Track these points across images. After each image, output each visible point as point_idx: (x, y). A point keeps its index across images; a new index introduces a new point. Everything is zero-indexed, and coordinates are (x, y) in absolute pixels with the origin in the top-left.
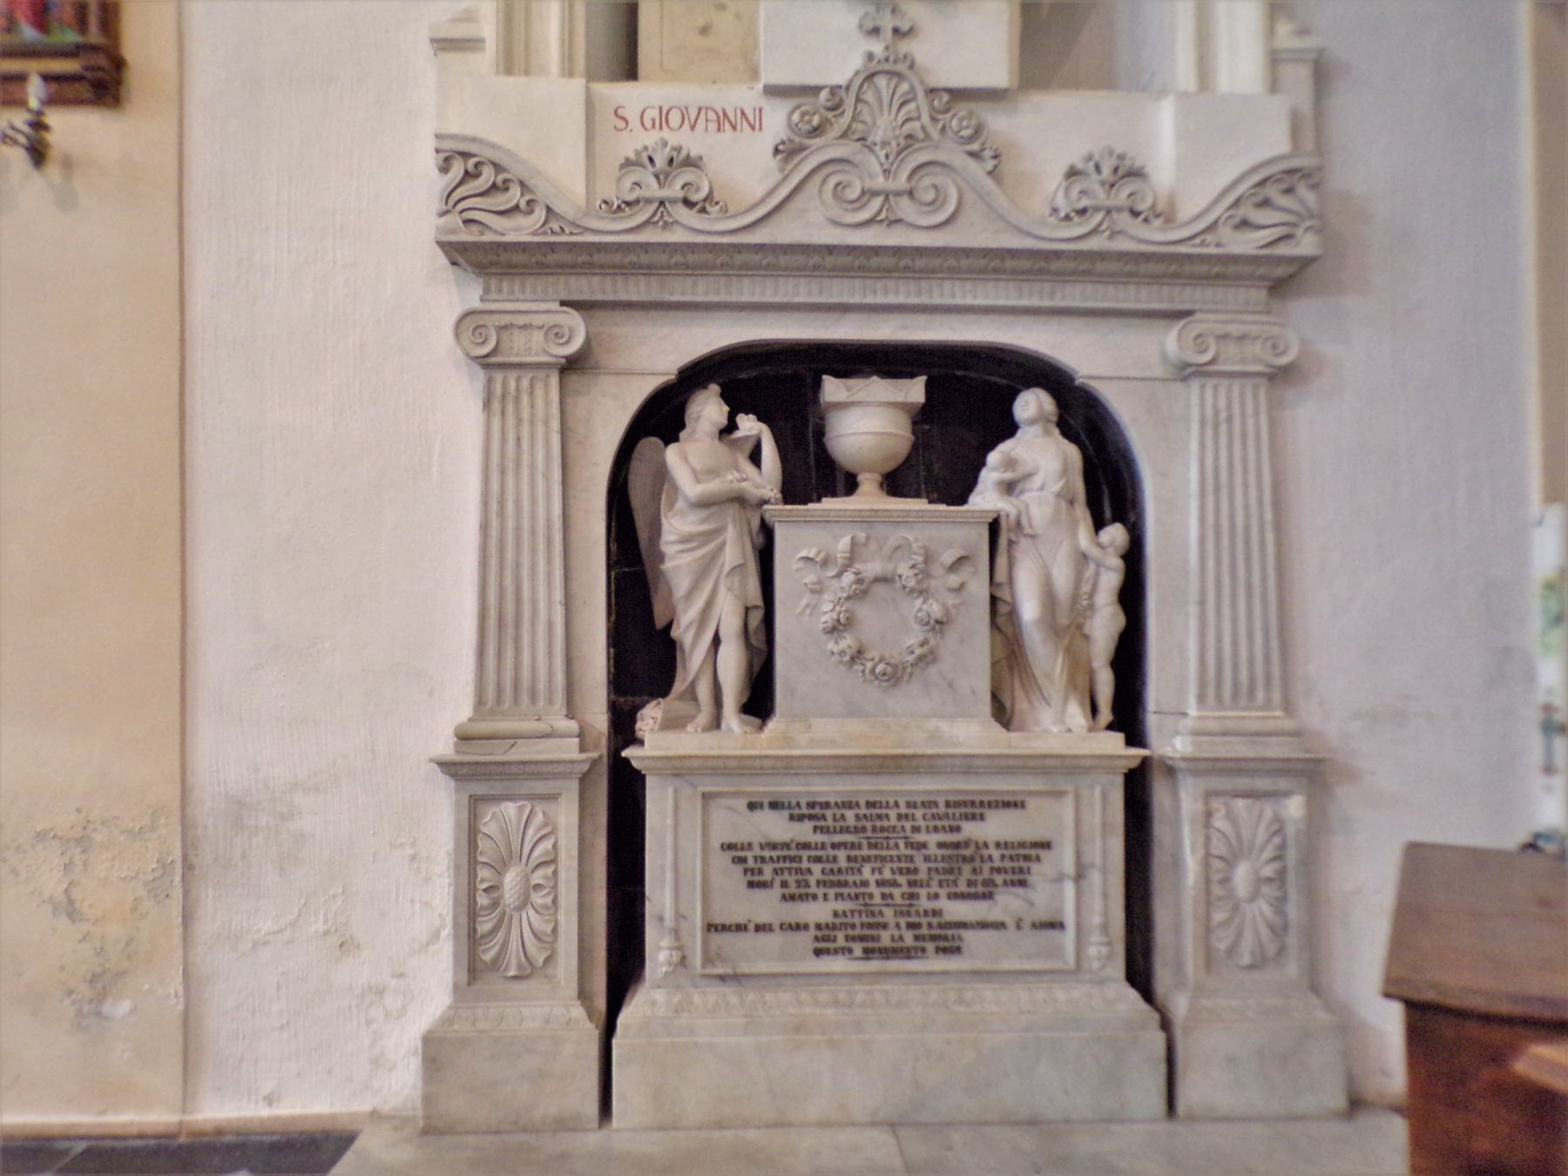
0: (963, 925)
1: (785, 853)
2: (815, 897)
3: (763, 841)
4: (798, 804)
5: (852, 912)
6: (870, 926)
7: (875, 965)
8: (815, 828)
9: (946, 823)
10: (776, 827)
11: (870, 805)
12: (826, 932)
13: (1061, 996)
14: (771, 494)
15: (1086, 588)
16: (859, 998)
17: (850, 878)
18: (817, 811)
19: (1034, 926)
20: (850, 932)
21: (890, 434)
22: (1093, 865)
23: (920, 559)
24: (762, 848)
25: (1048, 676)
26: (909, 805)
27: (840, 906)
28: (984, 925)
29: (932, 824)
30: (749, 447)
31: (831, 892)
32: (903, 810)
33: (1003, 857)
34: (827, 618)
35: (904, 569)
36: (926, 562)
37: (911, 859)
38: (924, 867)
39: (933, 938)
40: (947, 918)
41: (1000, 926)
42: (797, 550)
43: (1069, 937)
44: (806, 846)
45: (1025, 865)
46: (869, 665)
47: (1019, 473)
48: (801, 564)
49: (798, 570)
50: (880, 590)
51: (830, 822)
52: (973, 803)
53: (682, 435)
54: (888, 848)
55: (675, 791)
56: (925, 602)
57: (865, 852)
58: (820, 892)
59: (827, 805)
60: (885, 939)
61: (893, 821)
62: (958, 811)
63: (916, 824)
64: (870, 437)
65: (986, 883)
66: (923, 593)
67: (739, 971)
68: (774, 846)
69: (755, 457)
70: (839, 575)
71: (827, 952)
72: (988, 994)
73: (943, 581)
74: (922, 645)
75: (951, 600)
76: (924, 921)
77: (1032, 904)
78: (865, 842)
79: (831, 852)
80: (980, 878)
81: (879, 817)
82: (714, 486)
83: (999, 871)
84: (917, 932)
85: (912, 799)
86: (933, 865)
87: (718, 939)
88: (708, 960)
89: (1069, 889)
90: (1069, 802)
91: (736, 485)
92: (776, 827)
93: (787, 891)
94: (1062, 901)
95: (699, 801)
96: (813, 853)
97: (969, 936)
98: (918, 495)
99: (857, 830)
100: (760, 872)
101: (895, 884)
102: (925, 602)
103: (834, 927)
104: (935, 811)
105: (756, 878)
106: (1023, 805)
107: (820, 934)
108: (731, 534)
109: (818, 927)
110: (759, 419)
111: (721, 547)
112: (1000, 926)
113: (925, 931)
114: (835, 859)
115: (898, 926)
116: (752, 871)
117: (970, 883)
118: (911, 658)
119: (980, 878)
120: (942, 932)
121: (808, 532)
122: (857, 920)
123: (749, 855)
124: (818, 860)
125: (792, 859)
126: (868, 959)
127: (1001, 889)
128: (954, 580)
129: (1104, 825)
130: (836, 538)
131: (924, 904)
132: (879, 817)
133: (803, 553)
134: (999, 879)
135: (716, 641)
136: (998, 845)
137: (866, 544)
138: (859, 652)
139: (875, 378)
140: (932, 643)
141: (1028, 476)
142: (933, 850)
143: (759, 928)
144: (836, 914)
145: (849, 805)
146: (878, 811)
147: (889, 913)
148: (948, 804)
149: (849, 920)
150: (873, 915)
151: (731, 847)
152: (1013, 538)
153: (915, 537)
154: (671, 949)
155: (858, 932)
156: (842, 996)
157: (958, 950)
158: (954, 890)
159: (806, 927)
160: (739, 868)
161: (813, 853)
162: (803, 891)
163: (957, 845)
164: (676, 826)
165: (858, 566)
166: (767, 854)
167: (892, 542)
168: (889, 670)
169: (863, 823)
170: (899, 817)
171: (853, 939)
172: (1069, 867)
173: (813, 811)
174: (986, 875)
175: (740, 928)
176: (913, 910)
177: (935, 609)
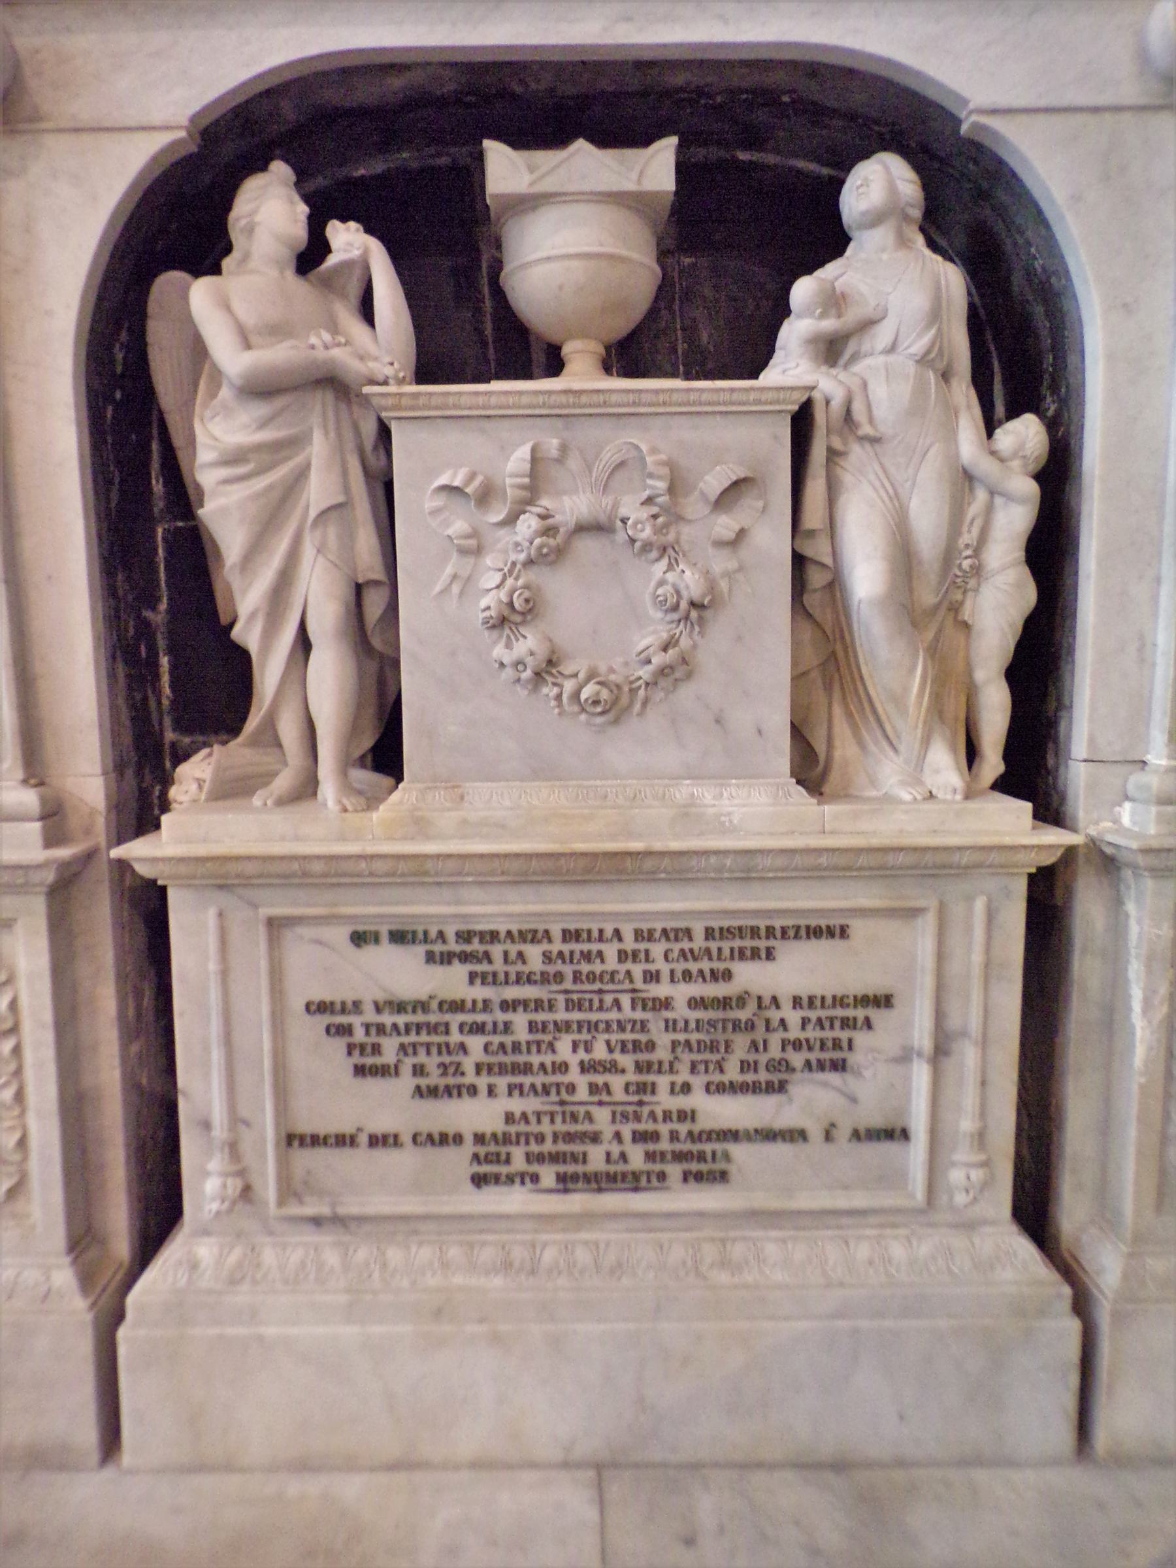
0: (733, 1135)
1: (420, 1018)
2: (473, 1091)
3: (381, 997)
4: (441, 934)
5: (539, 1115)
6: (570, 1137)
7: (577, 1201)
8: (472, 977)
9: (706, 965)
10: (403, 974)
11: (570, 936)
12: (493, 1148)
13: (898, 1251)
14: (389, 371)
15: (969, 537)
16: (549, 1256)
17: (535, 1060)
18: (476, 946)
19: (856, 1135)
20: (534, 1148)
21: (611, 257)
22: (964, 1034)
23: (661, 485)
24: (378, 1009)
25: (899, 701)
26: (638, 935)
27: (517, 1105)
28: (769, 1135)
29: (680, 967)
30: (354, 290)
31: (502, 1082)
32: (629, 944)
33: (805, 1022)
34: (491, 601)
35: (631, 508)
36: (671, 490)
37: (643, 1026)
38: (664, 1040)
39: (679, 1157)
40: (704, 1123)
41: (797, 1135)
42: (434, 473)
43: (918, 1150)
44: (457, 1006)
45: (844, 1035)
46: (569, 686)
47: (852, 316)
48: (440, 501)
49: (435, 512)
50: (588, 546)
51: (498, 965)
52: (754, 932)
53: (227, 263)
54: (601, 1009)
55: (220, 914)
56: (670, 567)
57: (561, 1015)
58: (482, 1082)
59: (494, 936)
60: (596, 1158)
61: (612, 963)
62: (726, 946)
63: (652, 967)
64: (576, 263)
65: (772, 1066)
67: (342, 1211)
68: (400, 1007)
69: (366, 311)
70: (511, 520)
71: (497, 1179)
72: (772, 1250)
73: (706, 527)
75: (720, 563)
76: (664, 1129)
77: (854, 1100)
78: (561, 998)
79: (501, 1017)
80: (763, 1059)
81: (587, 957)
82: (277, 355)
83: (797, 1045)
84: (651, 1147)
85: (645, 926)
86: (681, 1037)
87: (305, 1159)
88: (288, 1191)
89: (921, 1075)
90: (928, 924)
91: (321, 354)
92: (403, 974)
93: (423, 1082)
94: (907, 1095)
95: (262, 931)
96: (468, 1018)
97: (738, 1151)
99: (545, 979)
100: (376, 1049)
101: (613, 1068)
102: (670, 567)
103: (506, 1139)
104: (686, 945)
105: (369, 1061)
106: (843, 932)
107: (482, 1151)
108: (319, 448)
109: (479, 1139)
110: (369, 230)
111: (302, 474)
112: (797, 1135)
113: (665, 1145)
114: (507, 1027)
115: (618, 1136)
116: (362, 1047)
117: (745, 1066)
118: (645, 673)
119: (763, 1059)
120: (696, 1148)
121: (451, 438)
122: (546, 1128)
123: (356, 1021)
124: (479, 1029)
125: (432, 1029)
126: (566, 1191)
127: (798, 1076)
128: (725, 525)
129: (987, 965)
130: (505, 450)
131: (665, 1100)
132: (587, 957)
133: (443, 480)
134: (797, 1059)
135: (304, 643)
136: (797, 1002)
137: (560, 461)
138: (550, 662)
139: (581, 144)
140: (685, 642)
141: (867, 325)
142: (681, 1011)
143: (375, 1141)
144: (509, 1118)
145: (531, 936)
146: (586, 947)
147: (602, 1116)
148: (709, 933)
149: (534, 1128)
150: (574, 1117)
151: (322, 1008)
152: (837, 444)
153: (653, 442)
154: (225, 1175)
155: (548, 1147)
156: (518, 1254)
157: (723, 1176)
158: (717, 1077)
159: (458, 1139)
160: (340, 1043)
161: (468, 1018)
162: (451, 1080)
163: (724, 1003)
164: (225, 974)
165: (546, 502)
166: (387, 1019)
167: (609, 456)
168: (605, 694)
169: (559, 966)
170: (622, 956)
171: (540, 1158)
172: (922, 1036)
173: (468, 947)
174: (775, 1052)
175: (344, 1141)
176: (646, 1110)
177: (691, 582)
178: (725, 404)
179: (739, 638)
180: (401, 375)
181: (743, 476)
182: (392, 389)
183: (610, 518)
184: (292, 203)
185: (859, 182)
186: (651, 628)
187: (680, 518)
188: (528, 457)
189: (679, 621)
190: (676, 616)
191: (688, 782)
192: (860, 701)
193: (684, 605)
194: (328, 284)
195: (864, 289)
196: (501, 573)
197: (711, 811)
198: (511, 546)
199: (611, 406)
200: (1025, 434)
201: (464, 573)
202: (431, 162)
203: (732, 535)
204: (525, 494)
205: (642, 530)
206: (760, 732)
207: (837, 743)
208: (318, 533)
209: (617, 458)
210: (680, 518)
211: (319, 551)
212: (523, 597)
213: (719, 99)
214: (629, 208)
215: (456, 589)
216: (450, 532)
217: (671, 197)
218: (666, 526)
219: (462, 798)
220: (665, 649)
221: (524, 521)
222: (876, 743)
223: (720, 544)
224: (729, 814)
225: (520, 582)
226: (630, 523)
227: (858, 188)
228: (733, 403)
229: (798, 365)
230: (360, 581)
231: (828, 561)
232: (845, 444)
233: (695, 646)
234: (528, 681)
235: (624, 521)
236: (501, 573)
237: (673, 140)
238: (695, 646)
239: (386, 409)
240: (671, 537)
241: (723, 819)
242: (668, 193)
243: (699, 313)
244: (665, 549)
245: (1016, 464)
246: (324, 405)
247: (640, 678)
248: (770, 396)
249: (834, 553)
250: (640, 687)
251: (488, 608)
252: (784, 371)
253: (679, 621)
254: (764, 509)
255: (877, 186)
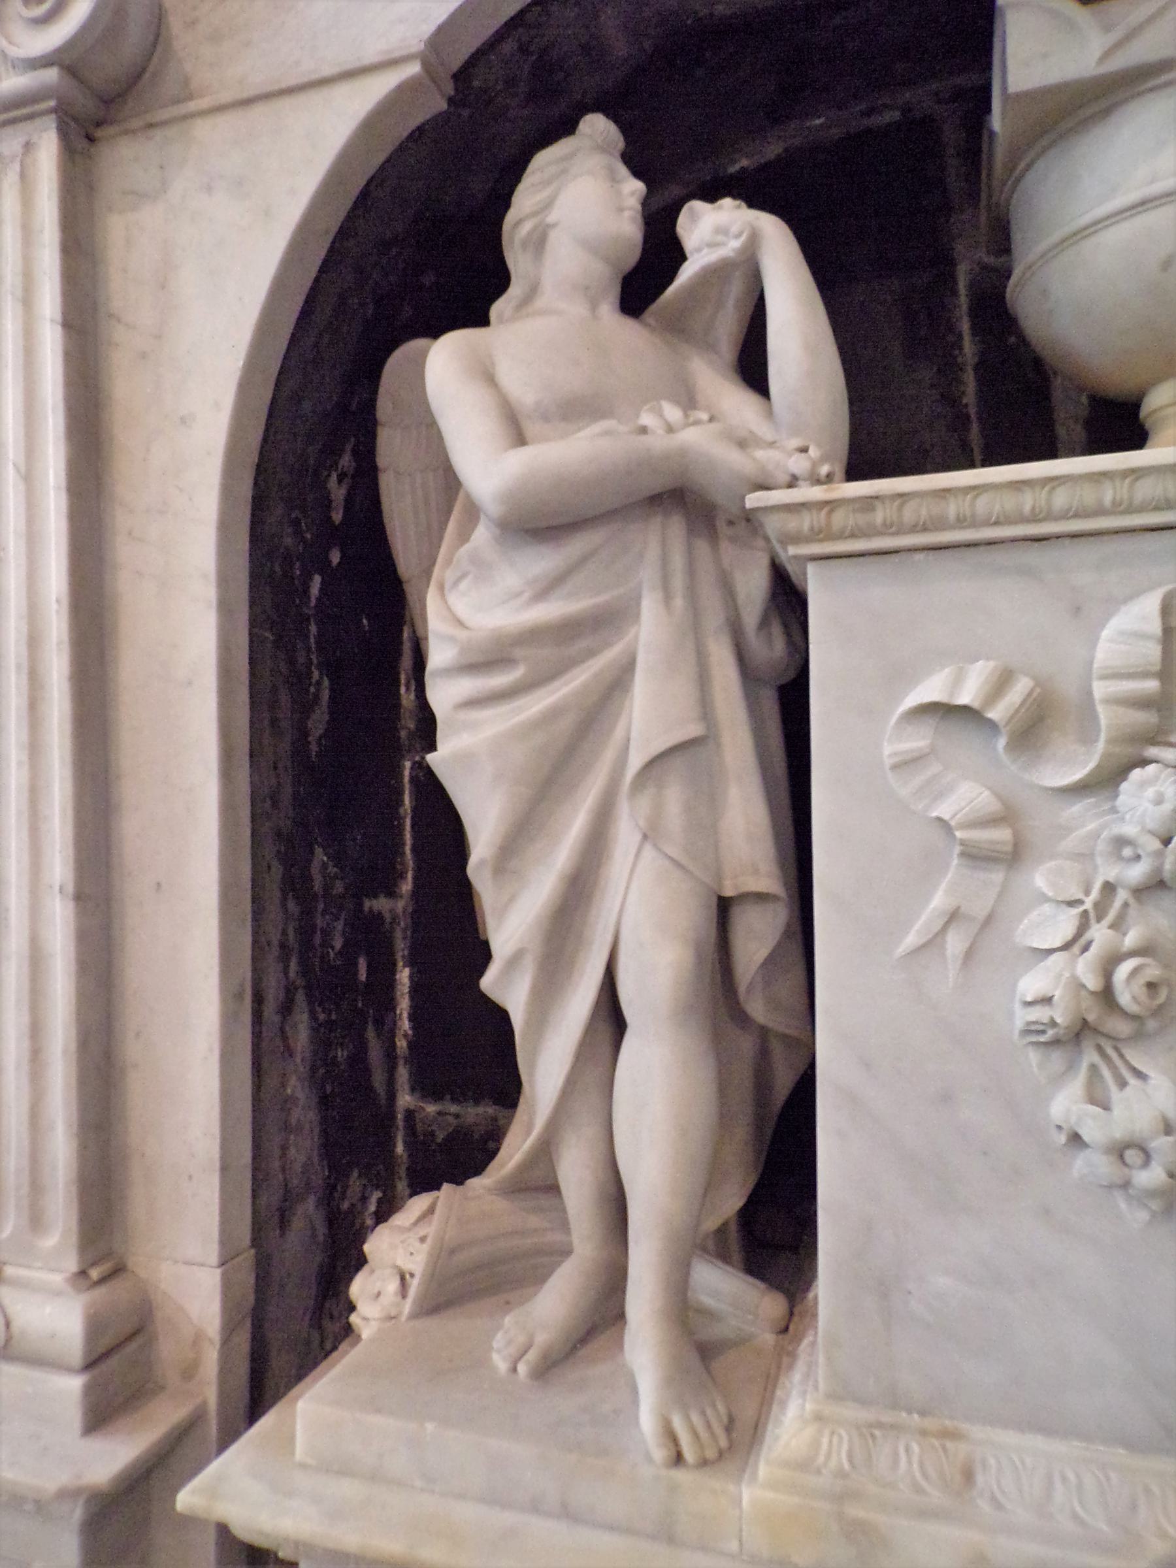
14: (798, 464)
30: (727, 328)
34: (1047, 983)
42: (907, 676)
48: (918, 740)
49: (907, 764)
53: (498, 309)
69: (752, 368)
70: (1107, 780)
82: (572, 453)
91: (658, 442)
108: (651, 630)
111: (617, 684)
130: (1084, 614)
133: (931, 690)
135: (611, 1016)
180: (824, 470)
182: (808, 493)
184: (614, 179)
188: (1155, 627)
194: (678, 328)
196: (1076, 911)
198: (1101, 846)
201: (979, 909)
202: (867, 122)
204: (1145, 718)
208: (644, 802)
211: (645, 837)
212: (1142, 980)
215: (955, 943)
216: (944, 810)
219: (968, 1475)
221: (1143, 784)
225: (1130, 940)
230: (728, 892)
234: (1153, 1193)
236: (1076, 911)
239: (796, 539)
246: (664, 543)
251: (1047, 1000)
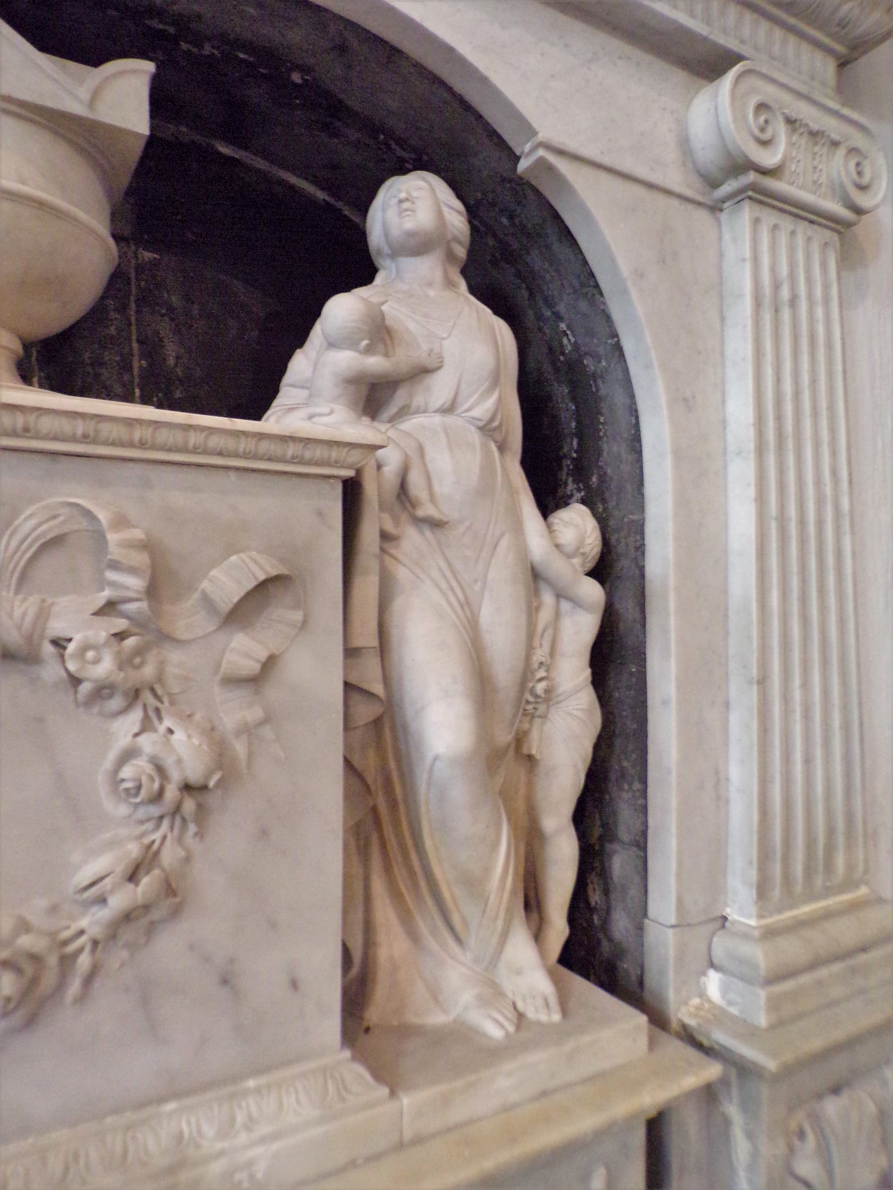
15: (540, 654)
23: (135, 583)
25: (474, 885)
35: (73, 618)
36: (152, 592)
56: (146, 726)
66: (141, 696)
74: (133, 877)
75: (234, 712)
98: (127, 397)
102: (146, 726)
118: (93, 921)
128: (243, 649)
140: (170, 856)
141: (422, 372)
152: (389, 527)
167: (30, 524)
177: (184, 749)
178: (245, 456)
179: (264, 833)
181: (274, 572)
183: (29, 639)
185: (403, 195)
186: (107, 836)
187: (165, 638)
189: (161, 818)
190: (155, 811)
191: (170, 1106)
192: (412, 873)
193: (172, 793)
195: (412, 326)
197: (216, 1168)
199: (37, 437)
200: (577, 524)
203: (256, 667)
205: (97, 661)
206: (294, 984)
207: (382, 937)
209: (50, 529)
210: (165, 638)
213: (207, 49)
214: (71, 143)
217: (137, 149)
218: (140, 651)
220: (133, 877)
222: (434, 932)
223: (232, 681)
224: (250, 1164)
226: (71, 647)
227: (401, 201)
228: (256, 457)
229: (332, 412)
231: (378, 689)
232: (397, 522)
233: (187, 860)
235: (59, 644)
237: (149, 67)
238: (187, 860)
240: (148, 671)
241: (238, 1177)
242: (137, 135)
243: (165, 328)
244: (137, 693)
245: (576, 561)
247: (82, 932)
248: (319, 452)
249: (386, 680)
250: (81, 950)
252: (311, 417)
253: (161, 818)
254: (304, 624)
255: (413, 207)
